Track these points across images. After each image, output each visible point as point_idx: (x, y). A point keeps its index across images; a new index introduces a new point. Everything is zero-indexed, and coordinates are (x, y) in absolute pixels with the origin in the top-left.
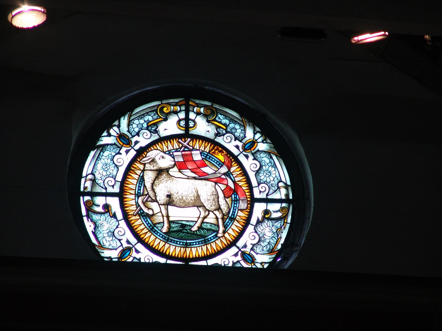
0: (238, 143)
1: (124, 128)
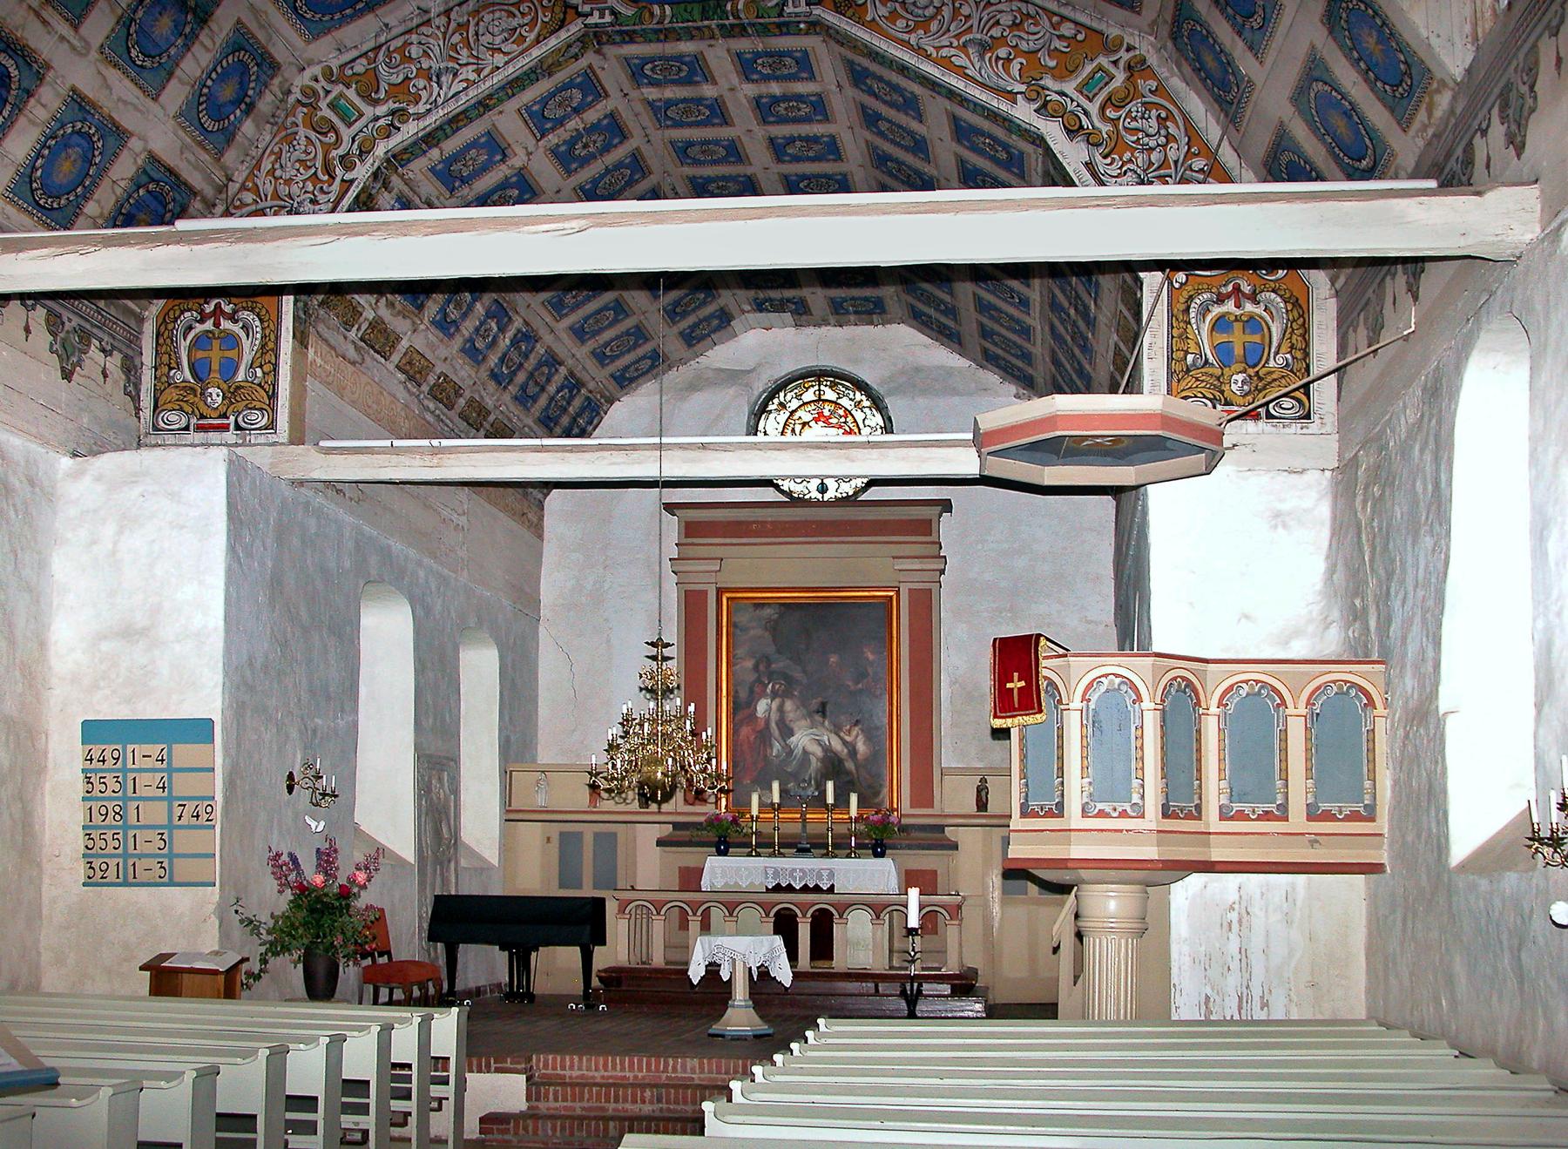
0: (851, 402)
1: (782, 399)
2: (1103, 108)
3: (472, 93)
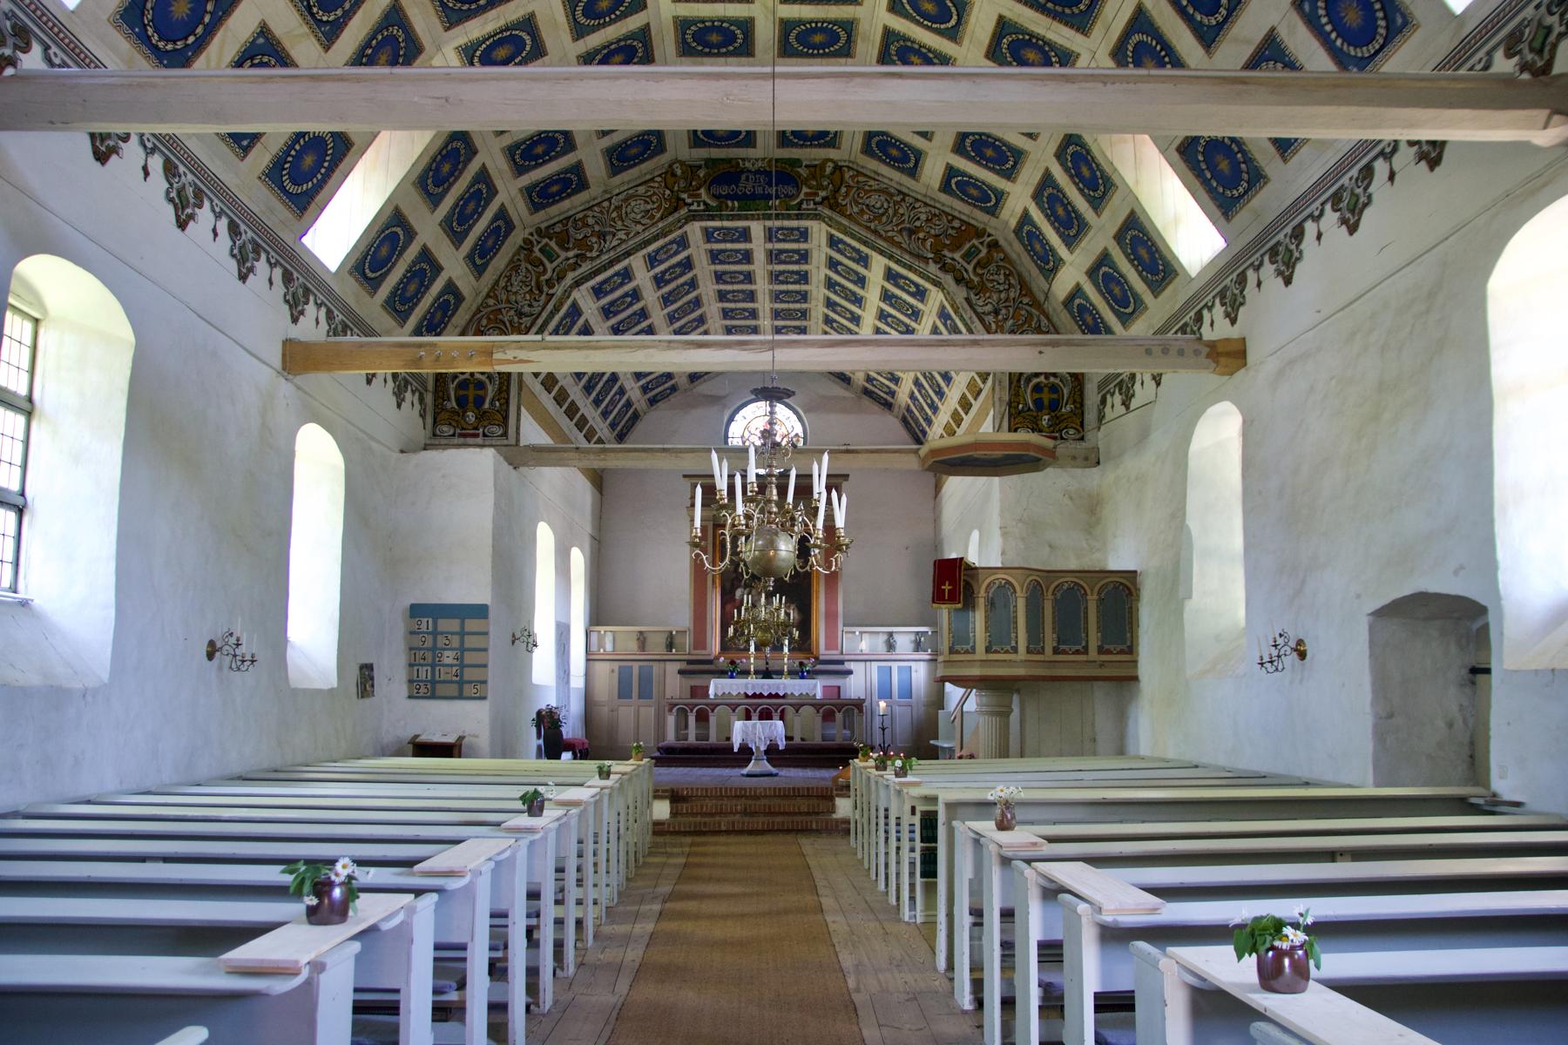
2: (975, 268)
3: (624, 246)
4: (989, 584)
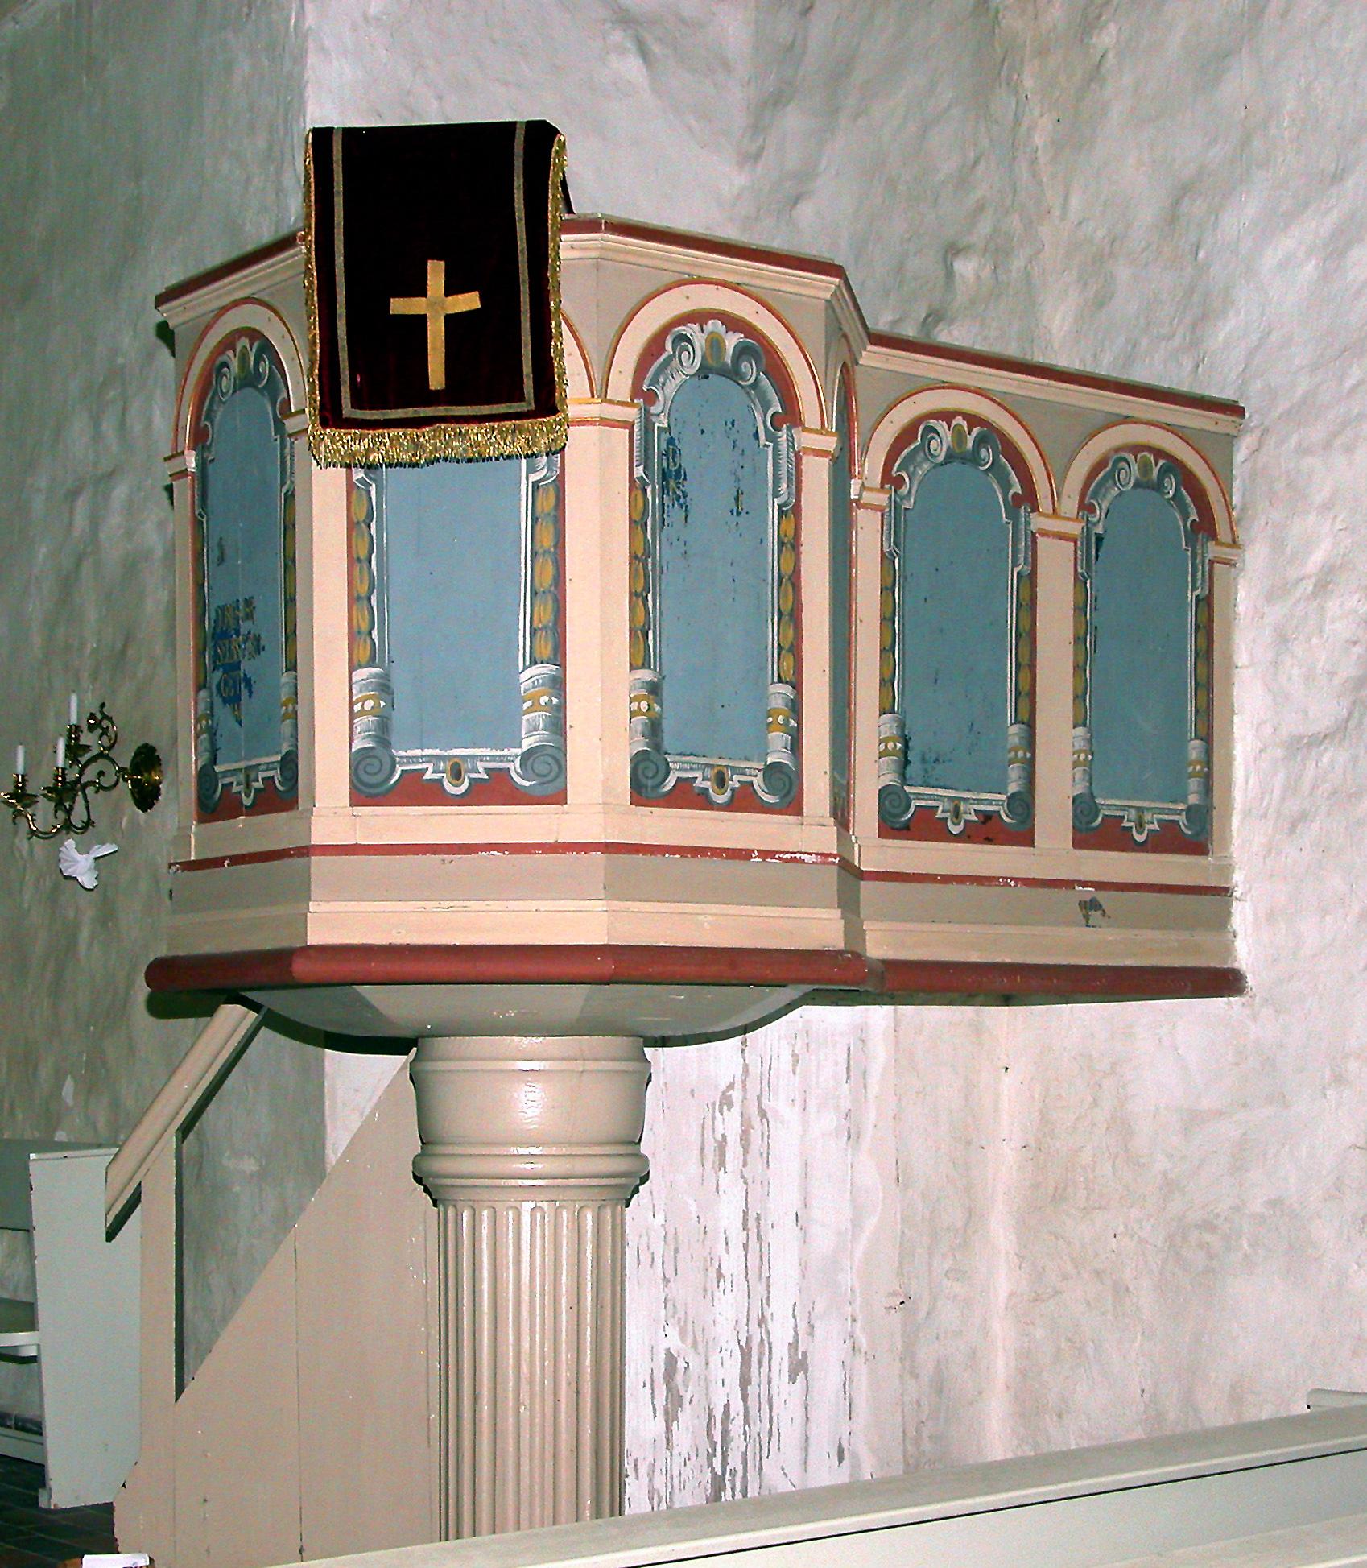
4: (654, 347)
